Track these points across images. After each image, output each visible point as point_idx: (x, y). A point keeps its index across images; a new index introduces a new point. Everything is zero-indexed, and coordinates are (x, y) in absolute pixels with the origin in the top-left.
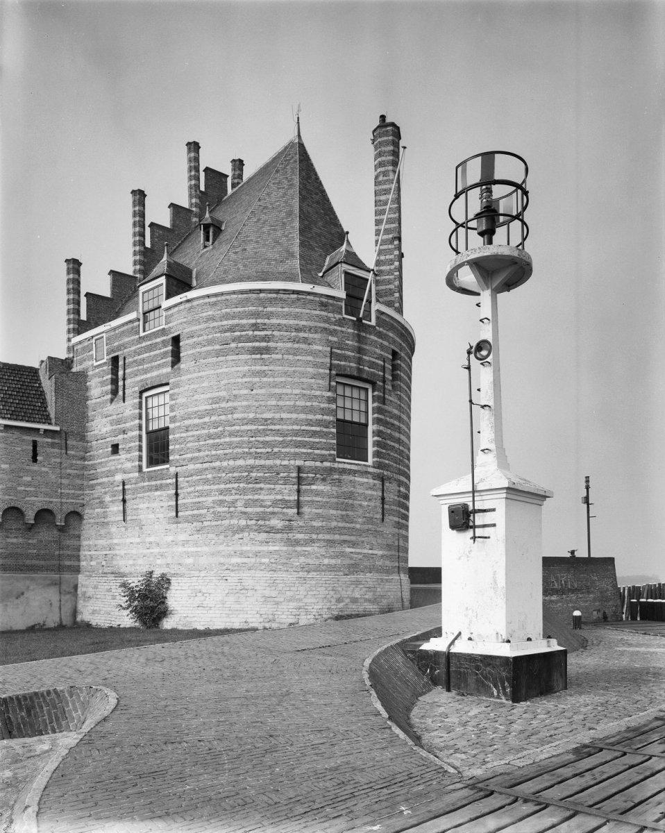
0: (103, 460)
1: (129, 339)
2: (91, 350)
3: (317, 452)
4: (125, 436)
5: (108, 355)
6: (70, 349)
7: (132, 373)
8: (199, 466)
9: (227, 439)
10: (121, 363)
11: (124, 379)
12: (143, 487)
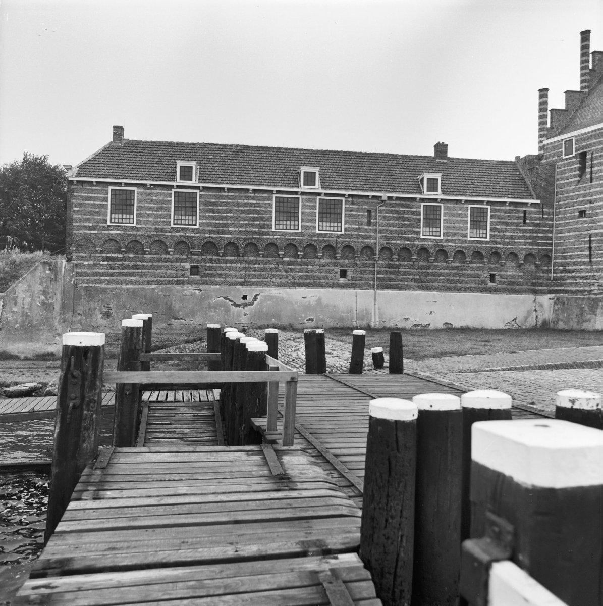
0: (570, 221)
1: (597, 140)
2: (562, 148)
4: (592, 205)
5: (576, 151)
6: (541, 148)
10: (588, 156)
11: (591, 168)
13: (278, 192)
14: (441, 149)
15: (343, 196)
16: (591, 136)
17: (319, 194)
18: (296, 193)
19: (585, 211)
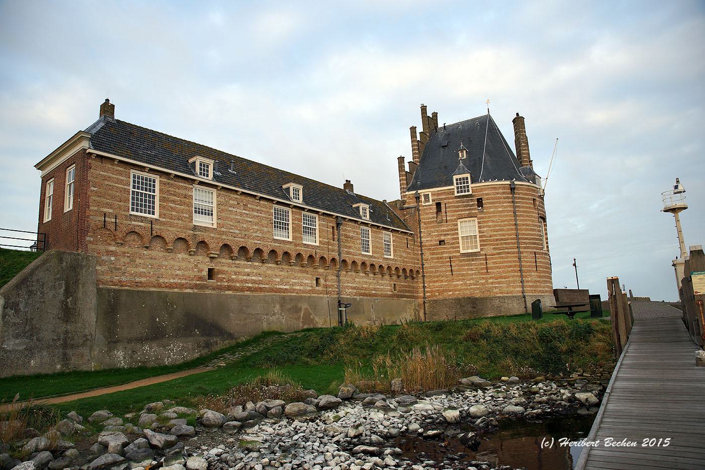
3: (539, 246)
7: (449, 211)
8: (499, 251)
9: (510, 241)
10: (443, 206)
12: (464, 260)
13: (278, 203)
14: (348, 184)
15: (317, 212)
16: (444, 193)
17: (303, 209)
18: (288, 205)
19: (444, 241)
